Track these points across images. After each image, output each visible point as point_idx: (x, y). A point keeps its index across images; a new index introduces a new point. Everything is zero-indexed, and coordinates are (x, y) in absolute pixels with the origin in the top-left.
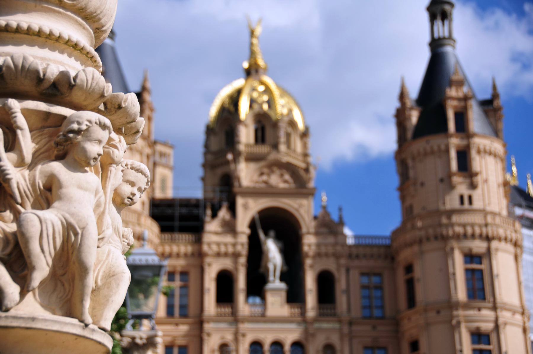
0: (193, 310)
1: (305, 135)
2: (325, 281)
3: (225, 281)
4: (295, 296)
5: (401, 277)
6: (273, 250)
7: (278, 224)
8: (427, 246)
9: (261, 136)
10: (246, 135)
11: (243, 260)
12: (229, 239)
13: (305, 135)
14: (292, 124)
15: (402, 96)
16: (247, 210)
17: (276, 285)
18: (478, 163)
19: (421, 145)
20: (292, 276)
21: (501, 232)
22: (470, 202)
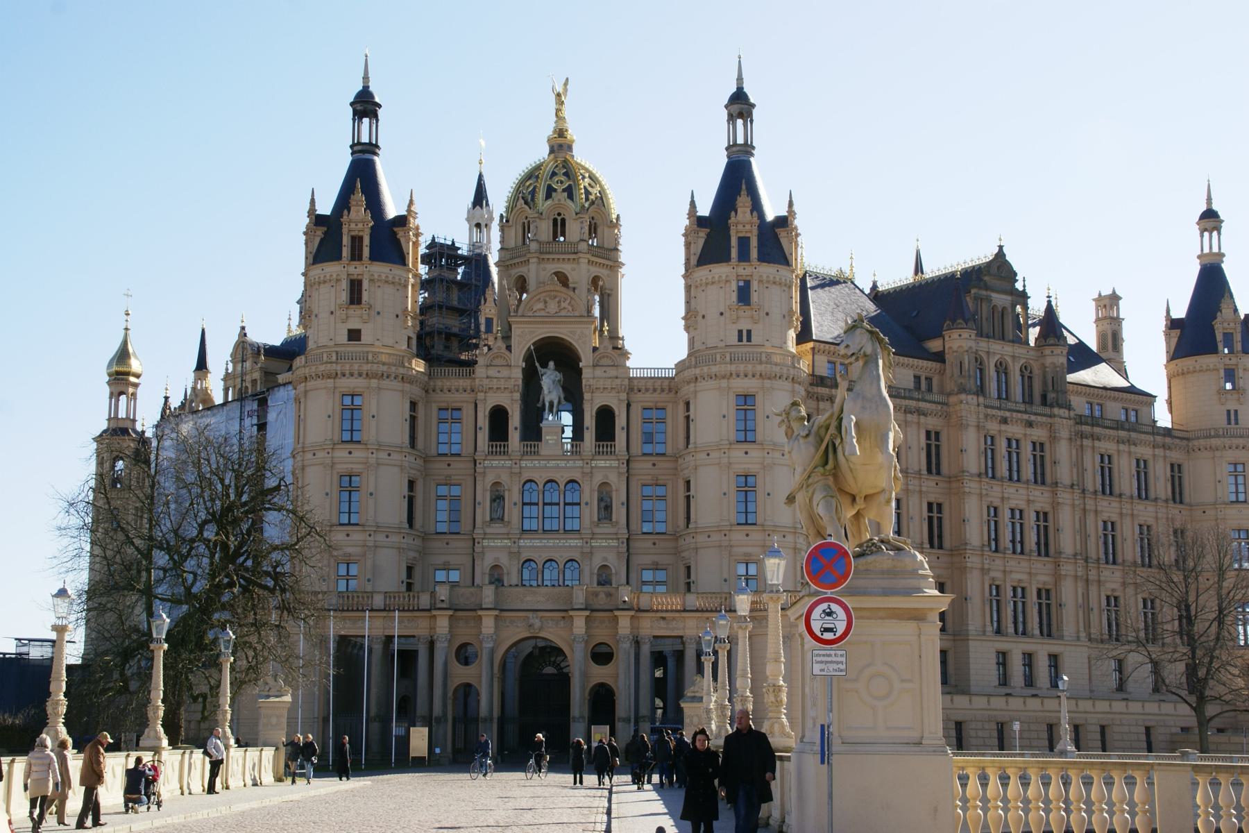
3: (499, 417)
6: (550, 380)
8: (702, 385)
11: (517, 396)
16: (525, 338)
22: (749, 340)
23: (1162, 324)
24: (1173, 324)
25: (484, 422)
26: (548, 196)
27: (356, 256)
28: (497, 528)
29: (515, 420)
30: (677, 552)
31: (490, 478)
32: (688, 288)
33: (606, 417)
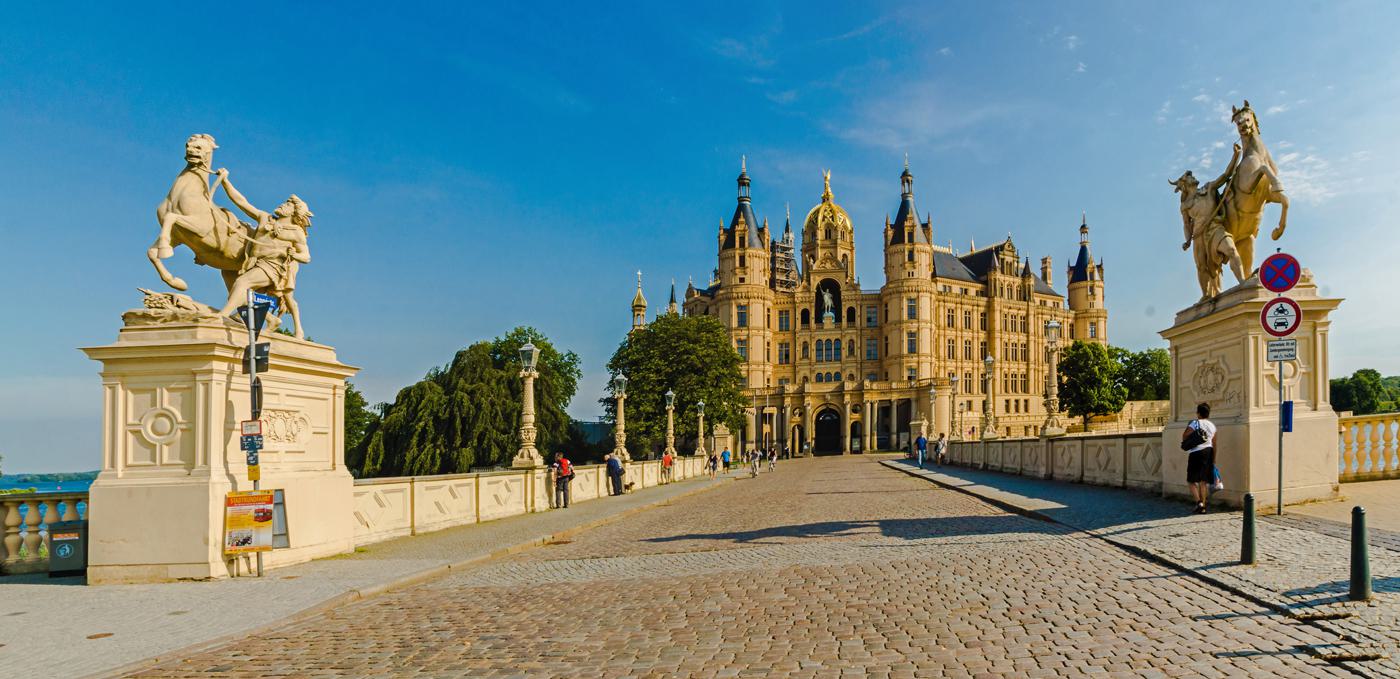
0: (791, 327)
1: (851, 232)
2: (851, 311)
3: (805, 314)
4: (838, 319)
5: (884, 309)
6: (827, 299)
7: (830, 285)
8: (893, 296)
9: (828, 234)
10: (821, 235)
11: (813, 304)
12: (808, 295)
13: (851, 232)
14: (845, 227)
15: (887, 224)
16: (816, 281)
17: (829, 315)
18: (916, 256)
19: (893, 248)
20: (837, 308)
21: (925, 289)
23: (1067, 269)
24: (1071, 269)
25: (799, 316)
26: (823, 220)
27: (742, 244)
28: (806, 361)
29: (813, 314)
30: (881, 367)
31: (802, 340)
32: (886, 255)
33: (851, 311)
